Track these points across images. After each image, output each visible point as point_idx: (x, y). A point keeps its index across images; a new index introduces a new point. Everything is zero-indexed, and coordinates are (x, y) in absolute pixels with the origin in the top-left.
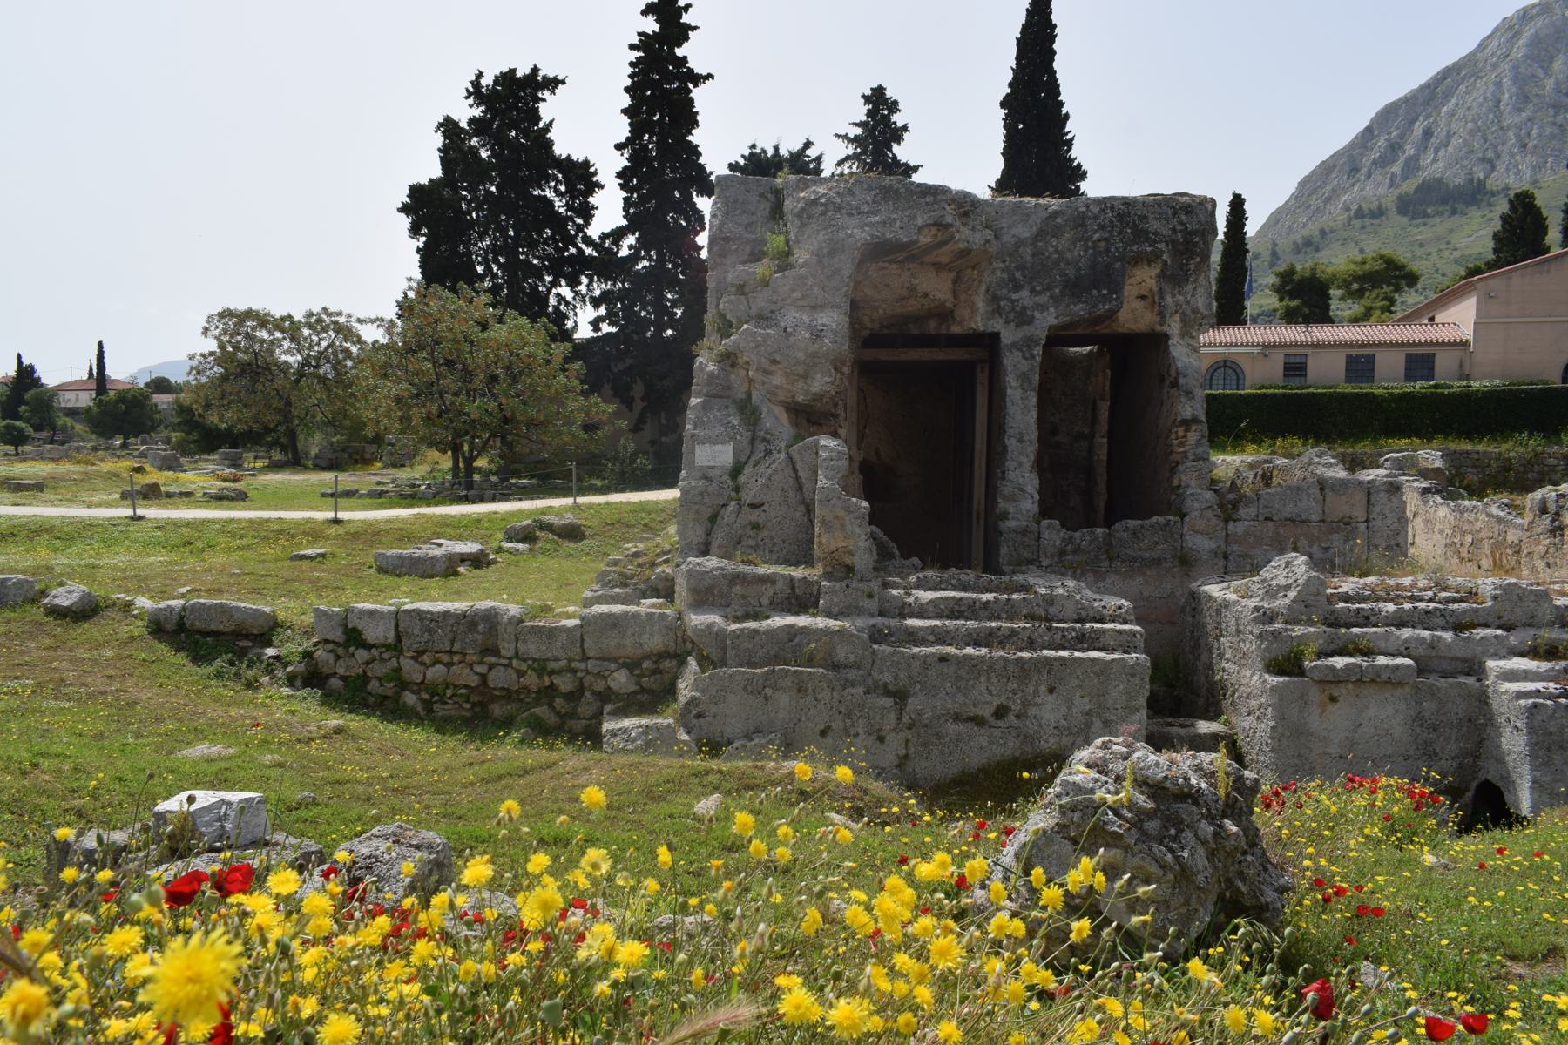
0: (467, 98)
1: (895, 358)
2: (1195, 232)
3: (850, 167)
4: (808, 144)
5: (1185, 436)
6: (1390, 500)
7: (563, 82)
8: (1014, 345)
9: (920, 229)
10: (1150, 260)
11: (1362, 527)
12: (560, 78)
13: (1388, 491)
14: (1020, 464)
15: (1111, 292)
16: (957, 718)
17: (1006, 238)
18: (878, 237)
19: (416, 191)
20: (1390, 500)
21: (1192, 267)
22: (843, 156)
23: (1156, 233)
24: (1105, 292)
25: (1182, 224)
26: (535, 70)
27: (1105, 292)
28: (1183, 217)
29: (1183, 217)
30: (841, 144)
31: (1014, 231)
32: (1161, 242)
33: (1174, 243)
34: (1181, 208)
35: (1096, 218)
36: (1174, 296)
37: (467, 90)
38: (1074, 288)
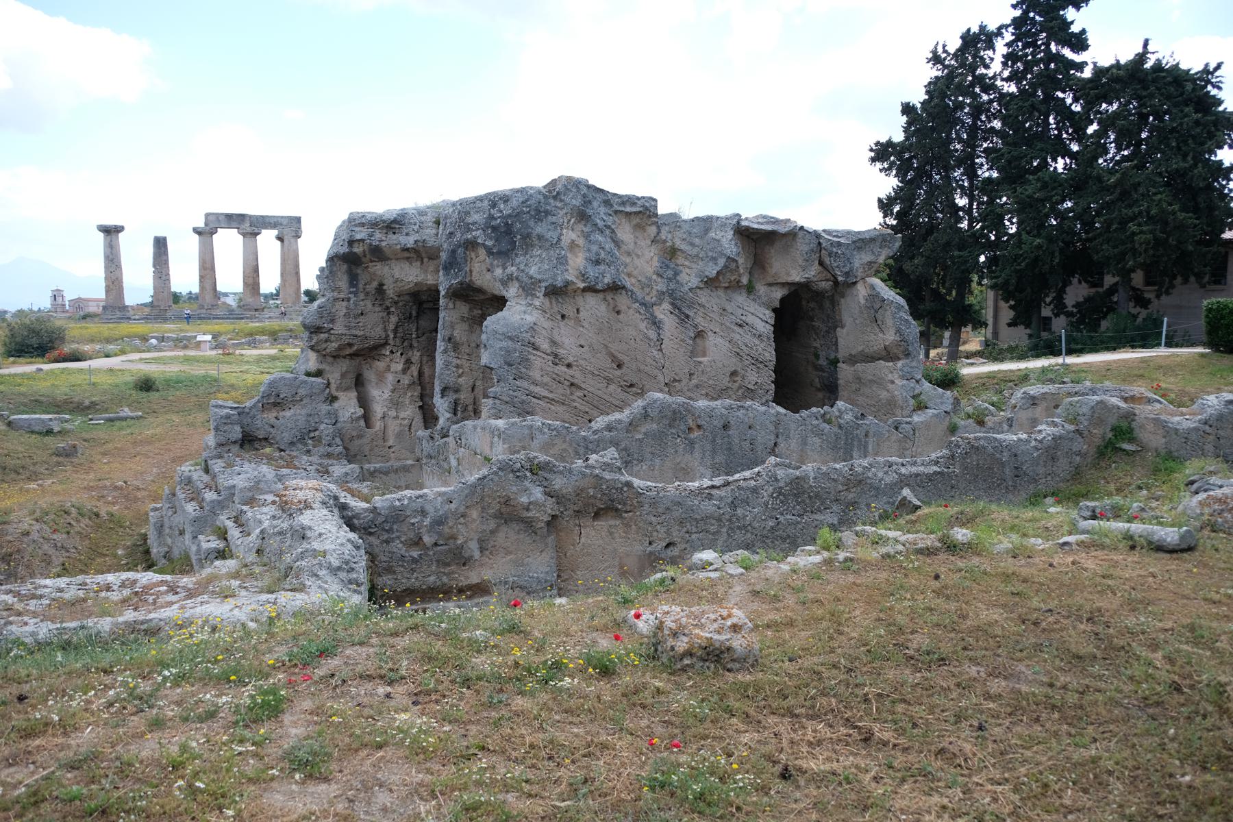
2: (510, 216)
19: (877, 143)
23: (475, 223)
25: (501, 212)
29: (502, 206)
33: (494, 228)
36: (504, 268)
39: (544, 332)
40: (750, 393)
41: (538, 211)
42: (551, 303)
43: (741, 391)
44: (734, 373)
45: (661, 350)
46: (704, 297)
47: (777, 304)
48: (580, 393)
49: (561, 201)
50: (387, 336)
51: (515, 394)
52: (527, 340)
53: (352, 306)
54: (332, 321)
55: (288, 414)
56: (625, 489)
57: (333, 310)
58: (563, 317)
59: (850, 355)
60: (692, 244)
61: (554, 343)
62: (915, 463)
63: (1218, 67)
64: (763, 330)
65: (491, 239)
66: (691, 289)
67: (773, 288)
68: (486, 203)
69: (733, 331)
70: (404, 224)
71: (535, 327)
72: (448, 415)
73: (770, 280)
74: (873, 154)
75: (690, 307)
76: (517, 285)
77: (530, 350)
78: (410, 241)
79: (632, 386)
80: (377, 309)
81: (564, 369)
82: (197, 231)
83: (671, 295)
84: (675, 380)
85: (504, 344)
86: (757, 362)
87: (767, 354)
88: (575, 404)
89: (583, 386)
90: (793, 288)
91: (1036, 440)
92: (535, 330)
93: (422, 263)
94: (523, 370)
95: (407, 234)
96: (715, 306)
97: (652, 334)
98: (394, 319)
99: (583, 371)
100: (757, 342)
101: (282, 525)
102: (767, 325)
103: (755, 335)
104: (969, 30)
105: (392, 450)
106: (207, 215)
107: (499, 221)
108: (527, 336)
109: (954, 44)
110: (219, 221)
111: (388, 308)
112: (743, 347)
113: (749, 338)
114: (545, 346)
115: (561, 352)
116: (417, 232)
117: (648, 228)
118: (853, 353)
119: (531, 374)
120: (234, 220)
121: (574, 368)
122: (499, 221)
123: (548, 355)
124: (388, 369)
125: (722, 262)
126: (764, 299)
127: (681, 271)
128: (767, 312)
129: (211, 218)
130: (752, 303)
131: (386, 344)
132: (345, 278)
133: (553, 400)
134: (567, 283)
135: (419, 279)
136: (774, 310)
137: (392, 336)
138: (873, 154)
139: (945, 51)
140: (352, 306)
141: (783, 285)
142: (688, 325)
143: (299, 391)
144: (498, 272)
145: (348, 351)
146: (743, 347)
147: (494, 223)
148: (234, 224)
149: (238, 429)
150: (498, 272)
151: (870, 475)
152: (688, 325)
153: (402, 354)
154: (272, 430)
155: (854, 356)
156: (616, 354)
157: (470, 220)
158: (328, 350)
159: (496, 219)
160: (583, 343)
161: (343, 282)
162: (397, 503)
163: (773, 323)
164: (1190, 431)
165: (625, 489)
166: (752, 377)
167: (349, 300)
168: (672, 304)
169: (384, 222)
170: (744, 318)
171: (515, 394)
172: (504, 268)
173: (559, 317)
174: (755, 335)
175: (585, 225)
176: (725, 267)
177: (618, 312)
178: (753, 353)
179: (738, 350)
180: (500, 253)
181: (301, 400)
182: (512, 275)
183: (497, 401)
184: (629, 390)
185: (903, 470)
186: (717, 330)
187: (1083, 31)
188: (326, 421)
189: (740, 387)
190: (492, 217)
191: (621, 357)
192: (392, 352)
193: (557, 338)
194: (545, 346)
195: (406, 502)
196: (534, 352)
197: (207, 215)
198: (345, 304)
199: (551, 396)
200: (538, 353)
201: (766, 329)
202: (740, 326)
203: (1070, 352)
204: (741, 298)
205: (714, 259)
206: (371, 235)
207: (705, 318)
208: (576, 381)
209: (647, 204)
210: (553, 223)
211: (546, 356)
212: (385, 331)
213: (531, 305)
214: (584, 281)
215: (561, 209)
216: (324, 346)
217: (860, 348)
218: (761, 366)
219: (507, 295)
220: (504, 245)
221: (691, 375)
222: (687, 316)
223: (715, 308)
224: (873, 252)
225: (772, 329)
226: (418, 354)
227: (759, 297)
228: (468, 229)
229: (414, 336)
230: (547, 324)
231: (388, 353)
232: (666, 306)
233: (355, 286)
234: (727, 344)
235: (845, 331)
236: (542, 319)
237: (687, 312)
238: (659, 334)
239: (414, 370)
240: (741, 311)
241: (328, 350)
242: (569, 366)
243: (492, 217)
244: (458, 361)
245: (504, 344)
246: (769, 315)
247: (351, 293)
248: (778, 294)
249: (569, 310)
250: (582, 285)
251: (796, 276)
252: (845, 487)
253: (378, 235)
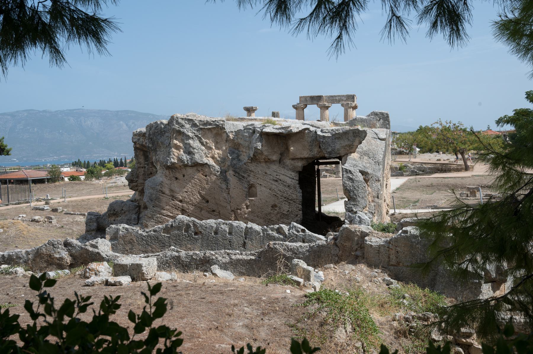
39: (166, 186)
40: (286, 218)
42: (169, 172)
43: (278, 216)
44: (274, 206)
46: (252, 167)
51: (154, 213)
52: (158, 189)
53: (146, 170)
54: (138, 177)
56: (97, 255)
57: (138, 172)
58: (177, 178)
61: (171, 190)
62: (241, 254)
64: (290, 183)
66: (245, 164)
67: (295, 161)
71: (162, 183)
73: (291, 157)
75: (244, 172)
77: (161, 194)
82: (294, 107)
83: (233, 167)
86: (287, 200)
90: (310, 161)
92: (162, 185)
94: (157, 203)
96: (260, 172)
97: (224, 186)
99: (187, 203)
100: (287, 189)
102: (293, 180)
103: (285, 186)
106: (300, 98)
108: (159, 188)
110: (306, 100)
113: (281, 187)
114: (167, 192)
119: (161, 205)
120: (316, 99)
126: (291, 167)
127: (241, 155)
128: (293, 173)
129: (302, 99)
130: (282, 169)
132: (142, 157)
134: (173, 164)
140: (146, 170)
141: (302, 159)
142: (244, 181)
143: (123, 209)
148: (315, 102)
149: (95, 224)
151: (214, 257)
152: (244, 181)
161: (142, 160)
162: (11, 253)
163: (297, 178)
164: (380, 246)
165: (97, 255)
166: (285, 208)
167: (145, 167)
168: (234, 171)
170: (278, 177)
171: (154, 213)
173: (174, 179)
174: (285, 186)
175: (183, 136)
178: (285, 195)
179: (275, 194)
181: (125, 213)
184: (212, 213)
185: (233, 257)
186: (262, 184)
189: (278, 213)
193: (173, 188)
194: (167, 192)
195: (14, 253)
196: (163, 195)
197: (300, 98)
198: (143, 169)
199: (171, 215)
200: (164, 195)
202: (276, 181)
204: (274, 167)
206: (139, 140)
207: (254, 178)
209: (217, 124)
211: (168, 197)
218: (291, 202)
222: (243, 177)
223: (260, 172)
224: (349, 140)
225: (297, 182)
227: (287, 166)
230: (168, 182)
233: (147, 161)
234: (268, 190)
236: (165, 180)
237: (243, 175)
240: (276, 174)
242: (181, 201)
246: (295, 176)
247: (145, 164)
248: (300, 165)
249: (180, 176)
252: (201, 263)
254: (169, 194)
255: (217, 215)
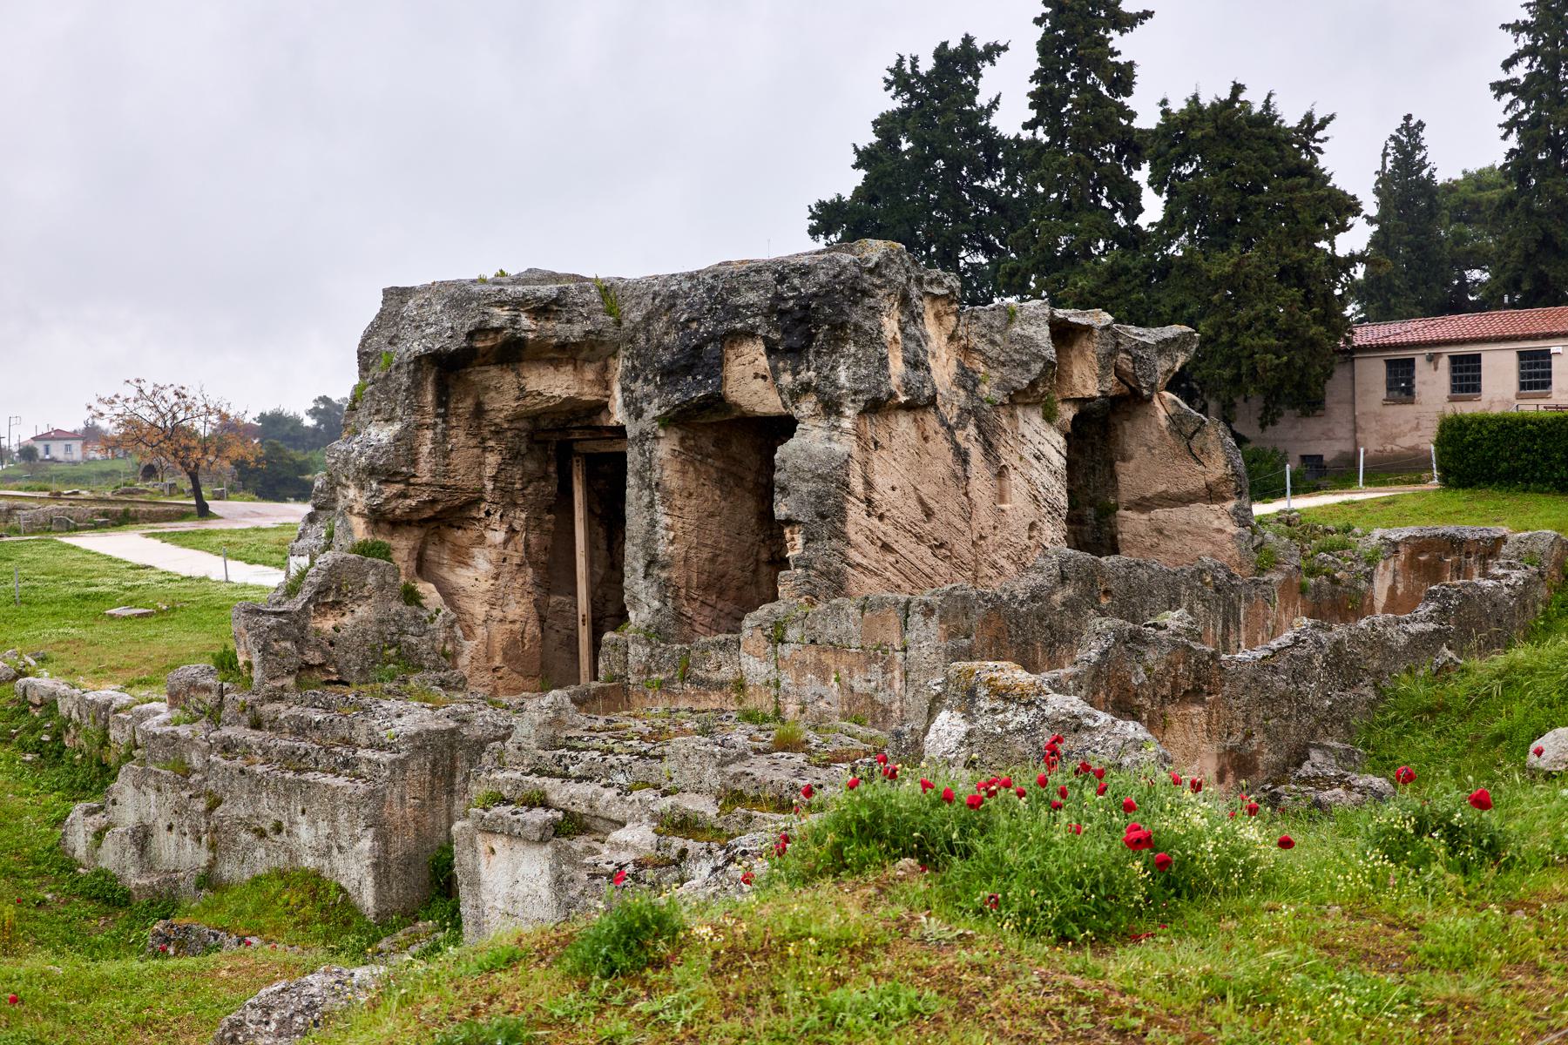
0: (887, 89)
1: (611, 450)
3: (1530, 66)
4: (1238, 89)
5: (793, 539)
6: (926, 624)
7: (1005, 48)
8: (634, 439)
9: (470, 335)
10: (750, 334)
11: (899, 656)
12: (1002, 44)
13: (924, 615)
14: (634, 570)
15: (707, 376)
16: (248, 827)
17: (626, 324)
18: (430, 349)
19: (821, 205)
20: (926, 624)
21: (821, 336)
22: (1513, 51)
23: (748, 306)
24: (700, 377)
25: (795, 289)
26: (968, 40)
27: (700, 377)
28: (796, 282)
30: (1509, 36)
31: (632, 316)
32: (757, 315)
33: (782, 313)
34: (793, 270)
35: (687, 295)
36: (795, 373)
37: (886, 81)
38: (671, 374)
41: (854, 290)
45: (966, 494)
47: (1068, 428)
48: (891, 558)
49: (881, 276)
50: (484, 486)
54: (414, 462)
55: (347, 619)
59: (1143, 498)
60: (993, 343)
63: (1324, 123)
64: (1058, 464)
65: (777, 330)
68: (768, 276)
69: (1032, 466)
70: (565, 305)
72: (656, 604)
73: (1067, 394)
74: (814, 222)
76: (814, 398)
78: (577, 330)
79: (941, 546)
80: (472, 443)
81: (875, 521)
84: (982, 537)
85: (812, 486)
87: (1062, 499)
88: (888, 574)
89: (895, 546)
91: (1507, 586)
93: (575, 369)
95: (569, 321)
98: (492, 459)
101: (1017, 719)
104: (944, 45)
105: (499, 675)
107: (791, 303)
109: (927, 65)
111: (484, 440)
112: (1041, 489)
115: (876, 496)
116: (588, 318)
117: (945, 318)
118: (1148, 495)
121: (886, 521)
122: (791, 303)
123: (862, 502)
124: (481, 540)
125: (1037, 367)
131: (483, 500)
133: (867, 568)
135: (572, 393)
136: (1067, 437)
137: (490, 486)
138: (814, 222)
139: (915, 73)
141: (1076, 401)
144: (786, 379)
145: (428, 513)
146: (1041, 489)
147: (782, 306)
150: (786, 379)
153: (501, 516)
154: (331, 649)
155: (1148, 500)
156: (925, 498)
157: (740, 301)
158: (398, 512)
159: (786, 300)
160: (895, 484)
168: (978, 427)
169: (540, 299)
170: (1041, 447)
172: (795, 373)
176: (1042, 374)
177: (926, 439)
178: (1050, 498)
179: (1036, 493)
180: (790, 350)
182: (809, 384)
183: (812, 573)
187: (1131, 64)
188: (411, 629)
190: (779, 297)
191: (932, 504)
192: (488, 513)
199: (865, 562)
201: (1059, 462)
202: (1038, 458)
203: (1296, 492)
205: (1025, 365)
206: (514, 321)
208: (888, 540)
210: (871, 308)
212: (480, 477)
213: (837, 428)
214: (906, 393)
215: (880, 287)
216: (393, 504)
217: (1162, 488)
219: (797, 414)
220: (795, 340)
221: (995, 528)
226: (523, 516)
228: (735, 312)
229: (518, 486)
231: (483, 515)
232: (972, 430)
235: (1132, 465)
238: (965, 470)
239: (520, 538)
241: (398, 512)
243: (779, 297)
244: (668, 520)
245: (812, 486)
246: (1059, 440)
247: (438, 415)
250: (903, 399)
251: (1092, 389)
253: (526, 321)
254: (862, 497)
255: (947, 557)
